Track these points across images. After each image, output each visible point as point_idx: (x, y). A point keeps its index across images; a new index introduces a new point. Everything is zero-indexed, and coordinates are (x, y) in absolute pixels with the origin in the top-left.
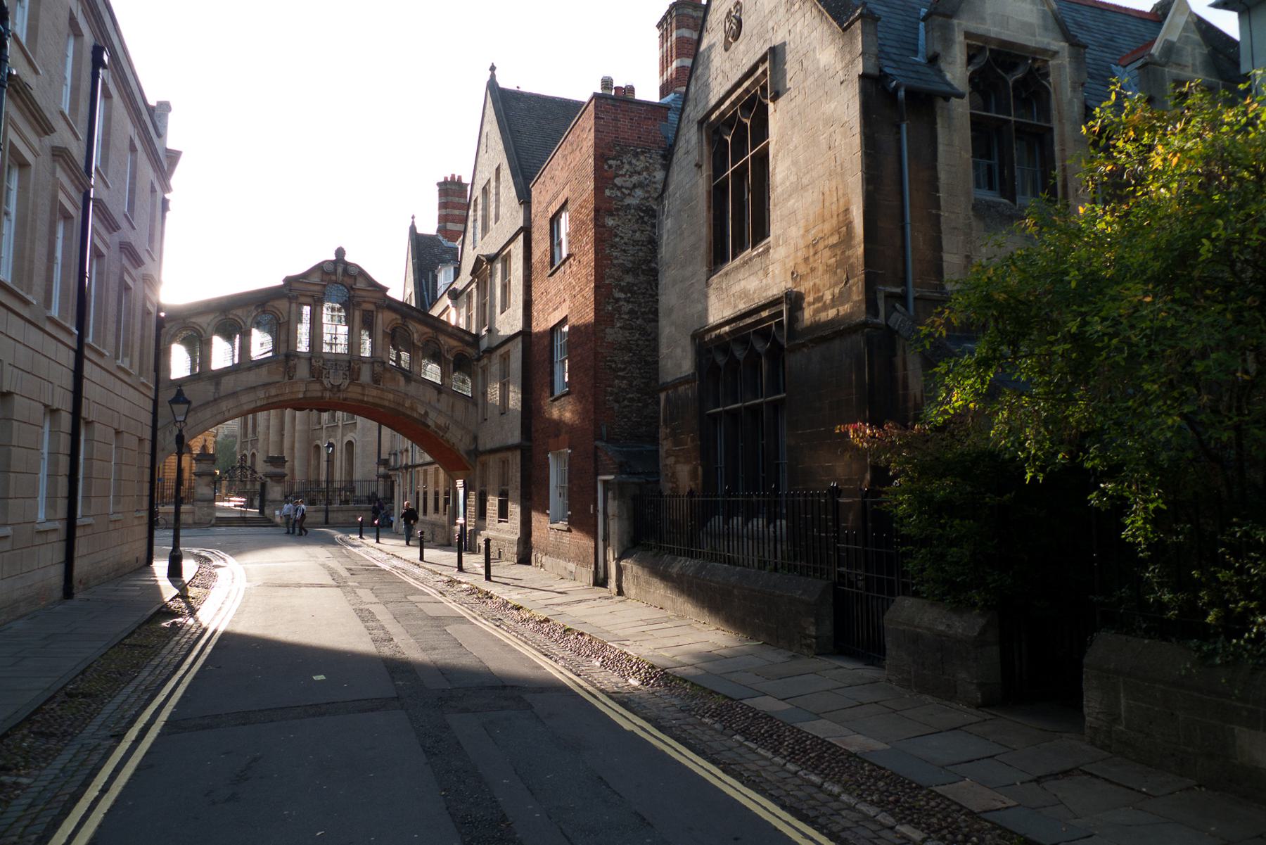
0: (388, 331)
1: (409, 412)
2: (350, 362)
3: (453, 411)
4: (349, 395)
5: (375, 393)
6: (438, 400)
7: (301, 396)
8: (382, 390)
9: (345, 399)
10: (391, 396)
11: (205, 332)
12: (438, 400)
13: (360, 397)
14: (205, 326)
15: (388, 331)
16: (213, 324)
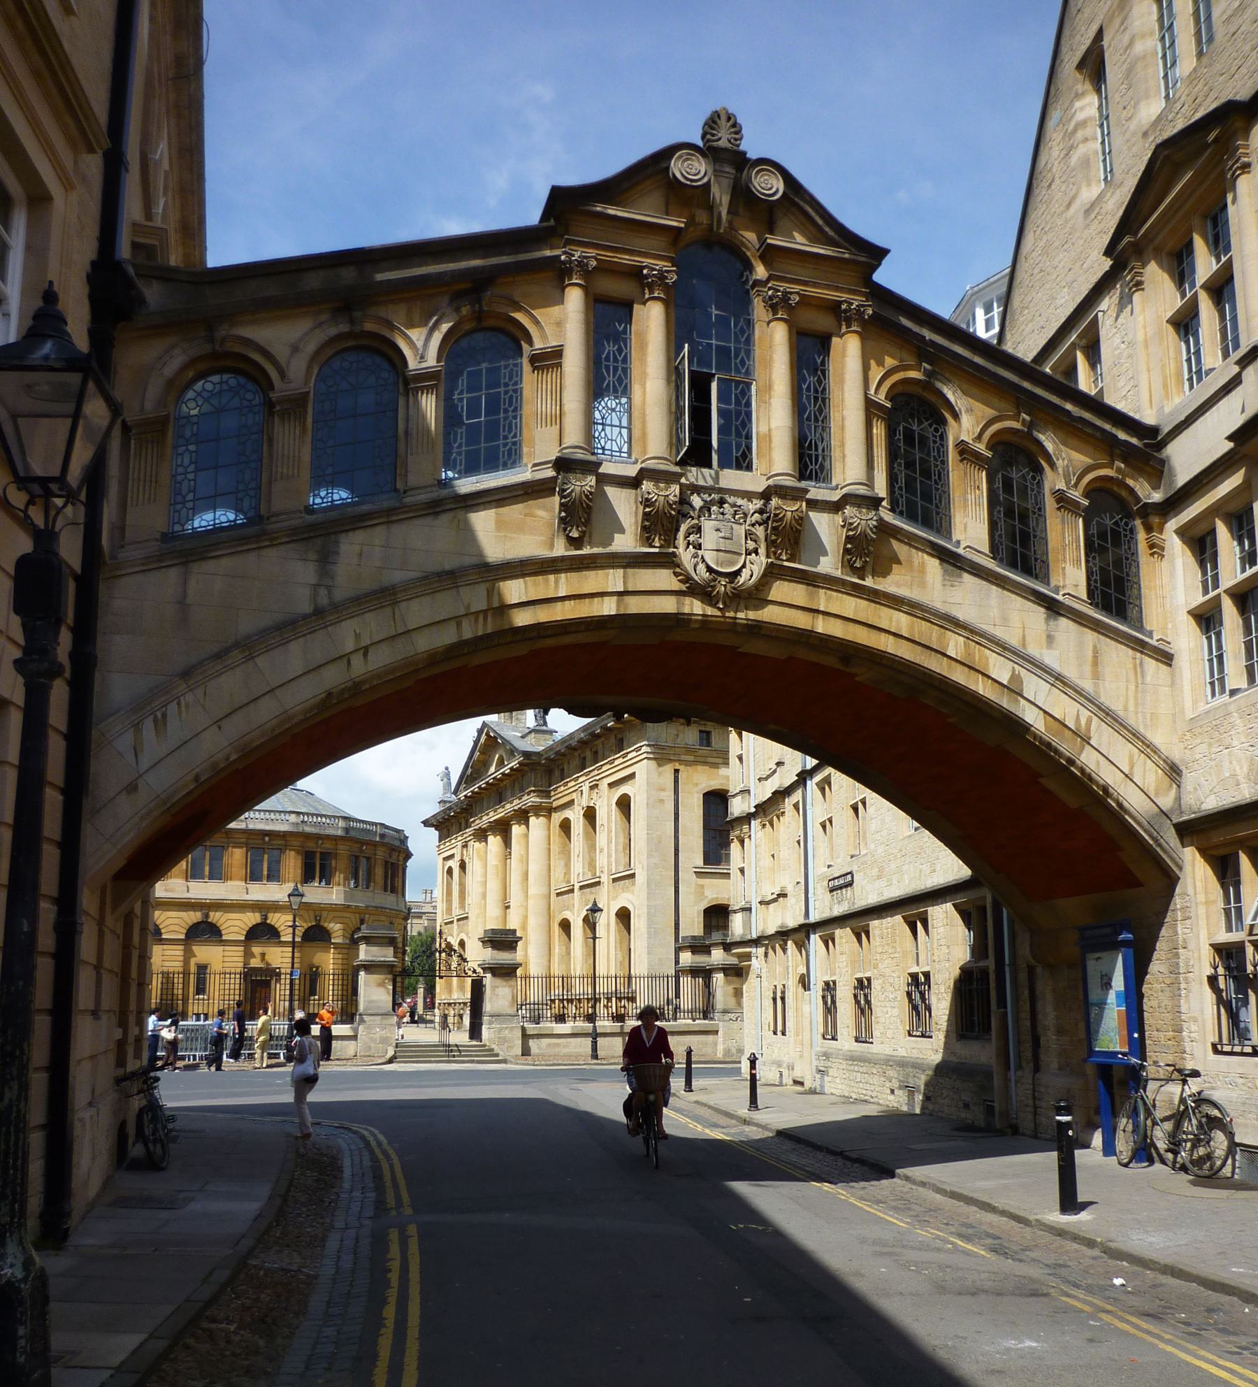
0: (881, 398)
1: (959, 676)
2: (766, 495)
3: (1096, 676)
4: (769, 614)
5: (850, 605)
6: (1050, 639)
7: (608, 607)
8: (875, 596)
9: (757, 628)
10: (900, 621)
11: (282, 374)
12: (1050, 639)
13: (801, 621)
14: (281, 353)
15: (881, 398)
16: (311, 347)
